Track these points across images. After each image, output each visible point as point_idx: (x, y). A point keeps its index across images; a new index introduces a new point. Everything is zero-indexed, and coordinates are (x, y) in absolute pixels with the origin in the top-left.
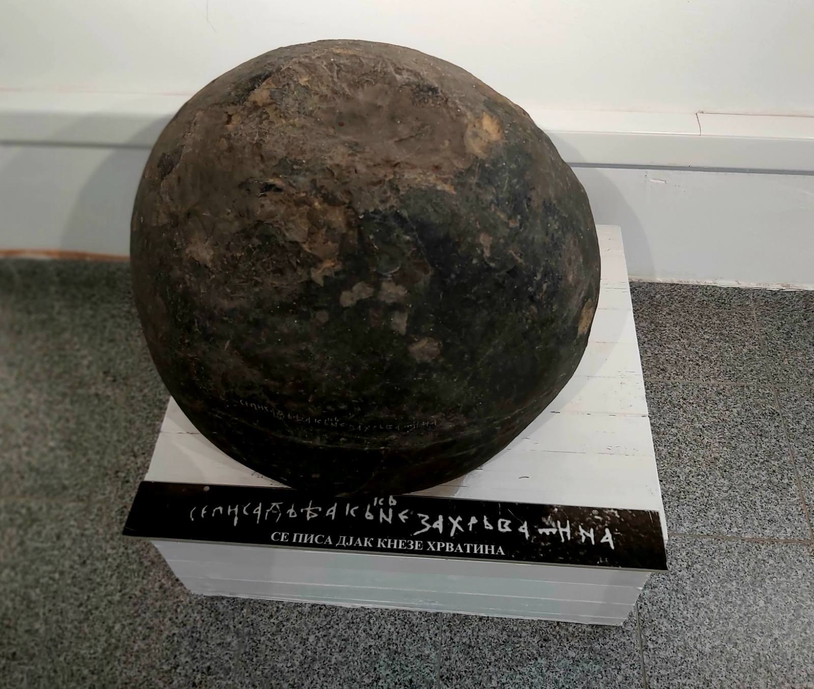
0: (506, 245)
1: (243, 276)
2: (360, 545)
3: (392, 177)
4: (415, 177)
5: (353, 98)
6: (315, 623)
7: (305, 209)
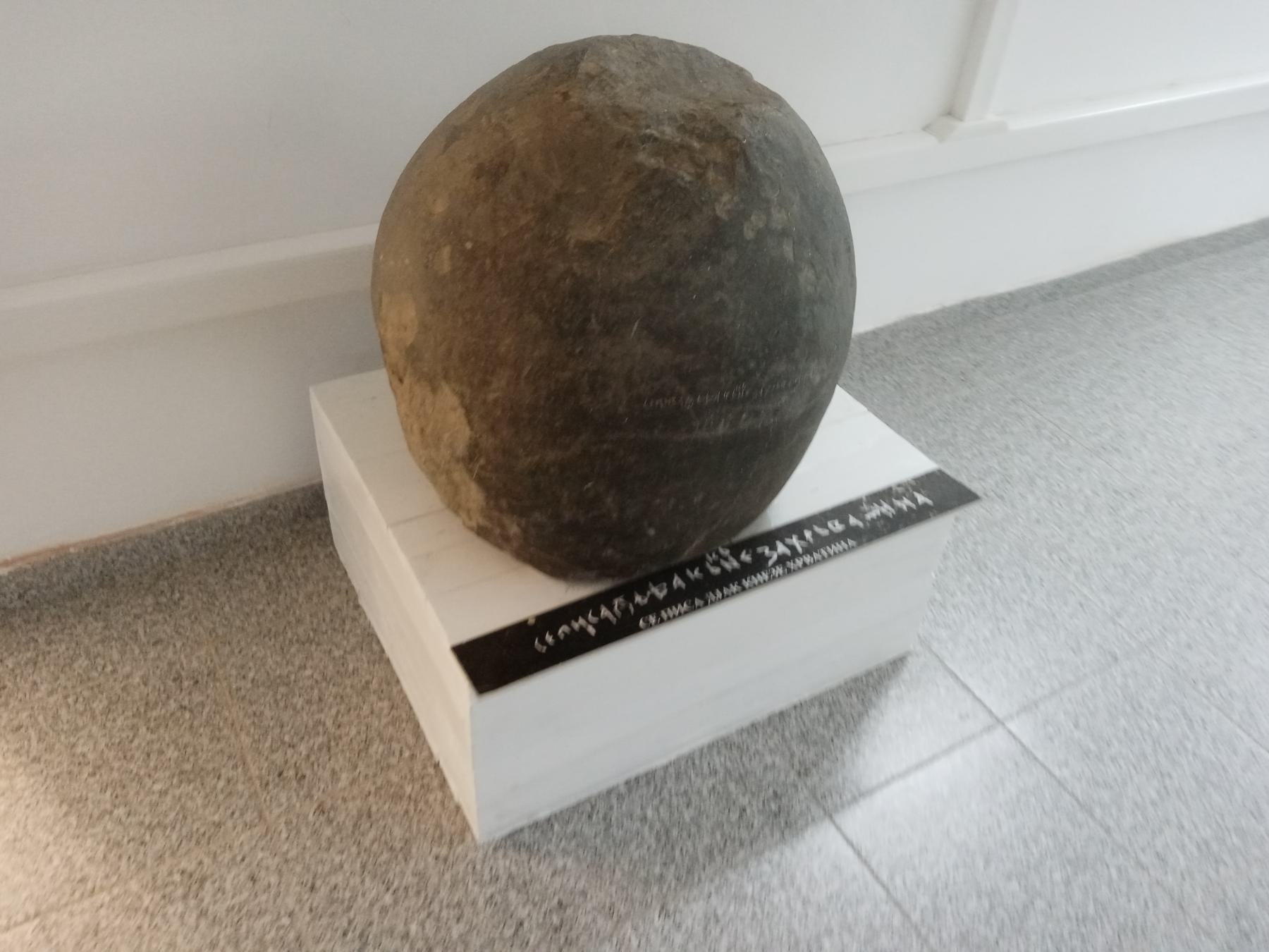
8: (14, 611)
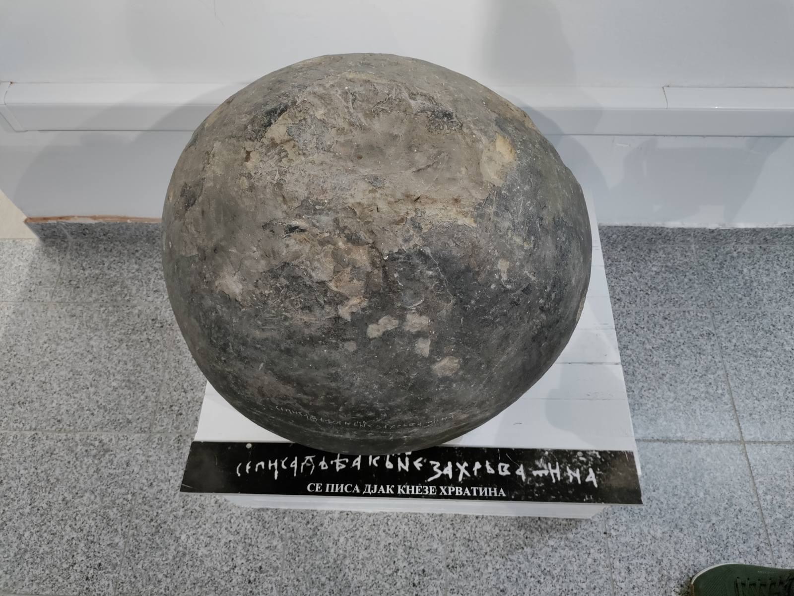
0: (522, 266)
1: (273, 312)
2: (384, 492)
3: (414, 214)
4: (438, 214)
5: (369, 129)
6: (344, 527)
7: (329, 248)
8: (102, 240)
